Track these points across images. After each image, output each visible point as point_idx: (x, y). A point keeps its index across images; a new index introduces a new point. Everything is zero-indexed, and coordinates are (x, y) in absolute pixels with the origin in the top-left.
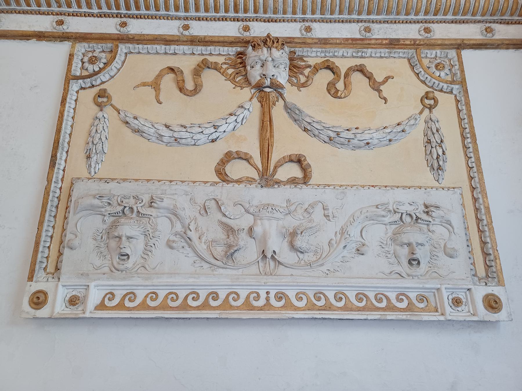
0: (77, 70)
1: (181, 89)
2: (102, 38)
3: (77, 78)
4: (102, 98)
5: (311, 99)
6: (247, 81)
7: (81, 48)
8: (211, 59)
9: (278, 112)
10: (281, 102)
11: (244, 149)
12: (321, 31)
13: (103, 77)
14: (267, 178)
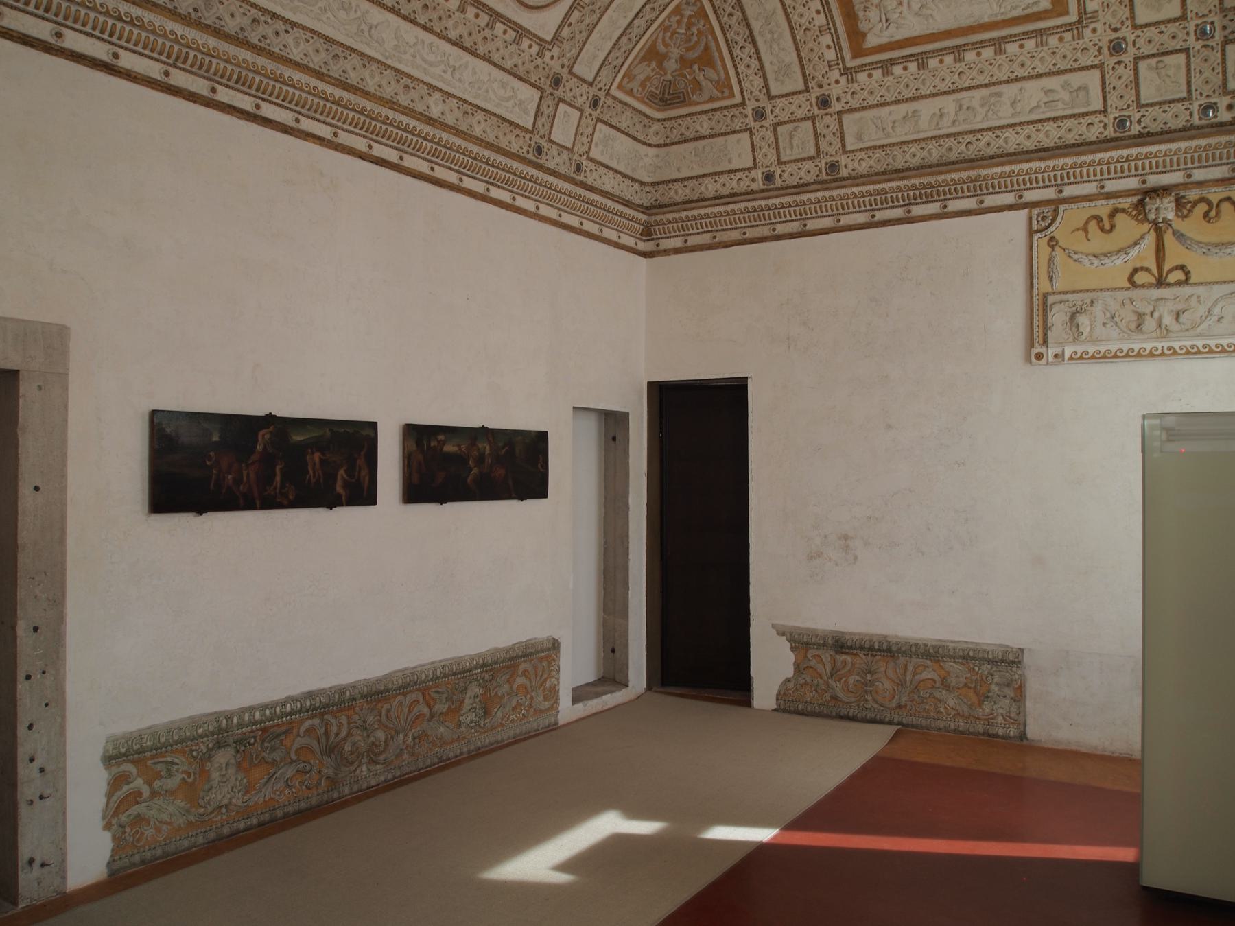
0: (1035, 227)
1: (1102, 229)
2: (1048, 202)
3: (1037, 232)
4: (1053, 242)
5: (1192, 226)
6: (1146, 219)
7: (1036, 211)
8: (1120, 206)
9: (1168, 238)
10: (1170, 231)
11: (1145, 264)
12: (1199, 175)
13: (1052, 229)
14: (1161, 283)
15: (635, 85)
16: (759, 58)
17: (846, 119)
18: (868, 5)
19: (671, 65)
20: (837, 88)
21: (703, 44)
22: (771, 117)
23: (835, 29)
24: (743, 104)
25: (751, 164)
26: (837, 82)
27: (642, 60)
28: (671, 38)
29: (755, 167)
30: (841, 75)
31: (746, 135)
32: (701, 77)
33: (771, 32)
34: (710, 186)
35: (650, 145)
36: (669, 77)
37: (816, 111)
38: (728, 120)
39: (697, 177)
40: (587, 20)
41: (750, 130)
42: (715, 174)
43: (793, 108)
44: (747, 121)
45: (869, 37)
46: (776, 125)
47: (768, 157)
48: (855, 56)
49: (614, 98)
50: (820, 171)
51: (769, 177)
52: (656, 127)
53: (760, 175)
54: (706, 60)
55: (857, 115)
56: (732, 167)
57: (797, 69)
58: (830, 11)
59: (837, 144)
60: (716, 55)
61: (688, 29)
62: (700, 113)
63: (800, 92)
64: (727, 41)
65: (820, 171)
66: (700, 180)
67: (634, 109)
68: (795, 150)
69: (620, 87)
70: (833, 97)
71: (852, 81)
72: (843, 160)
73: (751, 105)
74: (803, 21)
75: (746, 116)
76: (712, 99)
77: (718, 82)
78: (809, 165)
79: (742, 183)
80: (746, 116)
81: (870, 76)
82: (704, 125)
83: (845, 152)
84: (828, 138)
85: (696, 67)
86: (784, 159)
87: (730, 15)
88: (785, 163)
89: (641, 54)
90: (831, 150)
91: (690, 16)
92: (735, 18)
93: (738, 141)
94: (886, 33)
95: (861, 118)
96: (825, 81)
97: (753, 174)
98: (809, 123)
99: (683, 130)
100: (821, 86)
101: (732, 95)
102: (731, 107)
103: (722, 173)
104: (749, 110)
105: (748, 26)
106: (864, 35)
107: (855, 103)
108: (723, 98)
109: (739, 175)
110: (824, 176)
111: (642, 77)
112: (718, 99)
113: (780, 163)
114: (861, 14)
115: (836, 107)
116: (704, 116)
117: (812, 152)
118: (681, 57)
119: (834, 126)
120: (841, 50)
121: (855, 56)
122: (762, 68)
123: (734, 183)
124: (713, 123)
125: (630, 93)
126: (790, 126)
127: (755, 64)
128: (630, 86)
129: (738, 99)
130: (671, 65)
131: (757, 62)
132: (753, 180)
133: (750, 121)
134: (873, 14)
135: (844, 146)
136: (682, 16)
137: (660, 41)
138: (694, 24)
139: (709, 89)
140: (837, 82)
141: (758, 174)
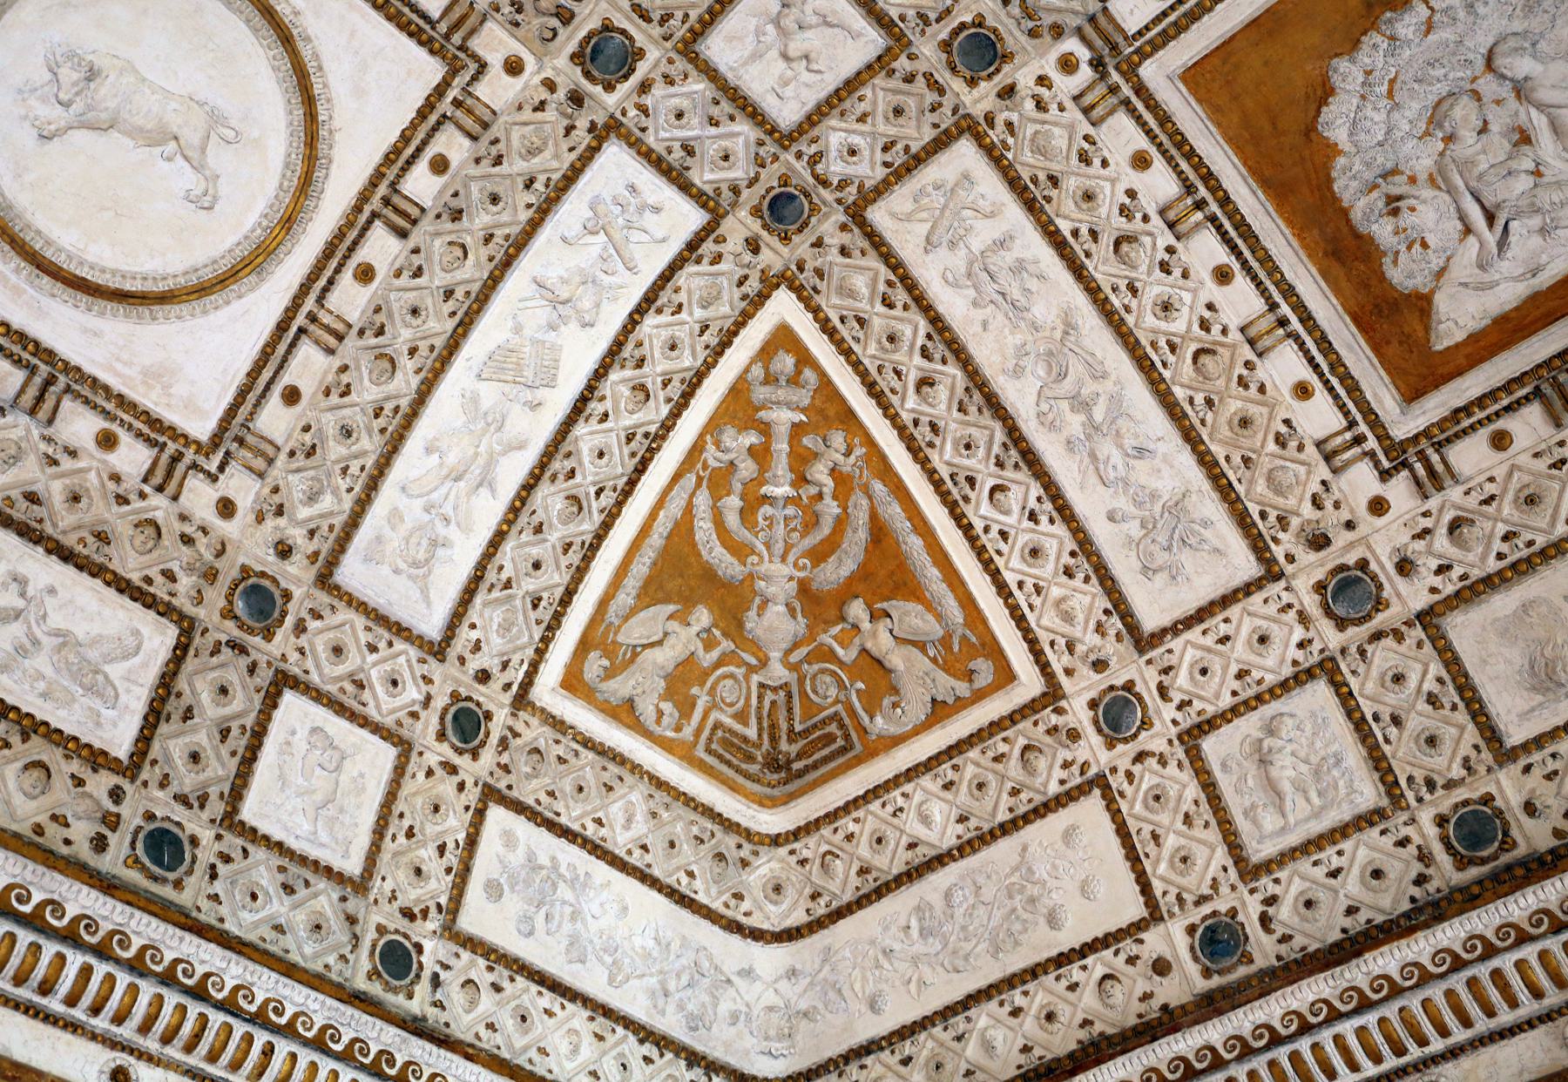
15: (643, 684)
16: (1064, 512)
17: (1462, 628)
18: (1398, 186)
19: (776, 625)
20: (1388, 524)
21: (861, 517)
22: (1169, 711)
23: (1307, 318)
24: (1052, 696)
25: (1135, 909)
26: (1378, 506)
27: (651, 593)
28: (747, 514)
29: (1155, 915)
30: (1385, 475)
31: (1091, 808)
32: (881, 641)
33: (1082, 405)
34: (999, 1036)
35: (757, 935)
36: (778, 672)
37: (1330, 637)
38: (1013, 767)
39: (946, 1014)
40: (367, 392)
41: (1101, 782)
42: (1011, 982)
43: (1240, 651)
44: (1081, 752)
45: (1442, 302)
46: (1192, 737)
47: (1194, 863)
48: (1412, 394)
49: (558, 725)
50: (1424, 857)
51: (1218, 940)
52: (768, 865)
53: (1182, 942)
54: (887, 576)
55: (1502, 603)
56: (1068, 939)
57: (1211, 507)
58: (1266, 260)
59: (1461, 735)
60: (914, 545)
61: (801, 480)
62: (911, 774)
63: (1248, 589)
64: (938, 484)
65: (1424, 857)
66: (959, 1022)
67: (660, 784)
68: (1297, 807)
69: (572, 682)
70: (1383, 564)
71: (1433, 481)
72: (1509, 788)
73: (1081, 691)
74: (1178, 325)
75: (1074, 735)
76: (940, 711)
77: (946, 641)
78: (1363, 850)
79: (1117, 992)
80: (1074, 735)
81: (1500, 441)
82: (933, 817)
83: (1505, 756)
84: (1413, 723)
85: (857, 610)
86: (1259, 851)
87: (925, 382)
88: (1267, 867)
89: (641, 568)
90: (1445, 763)
91: (797, 430)
92: (941, 393)
93: (1068, 835)
94: (1505, 267)
95: (1526, 607)
96: (1331, 519)
97: (1154, 942)
98: (1320, 691)
99: (864, 850)
100: (1319, 542)
101: (1006, 676)
102: (1013, 718)
103: (1034, 972)
104: (1078, 712)
105: (994, 405)
106: (1422, 304)
107: (1478, 561)
108: (979, 696)
109: (1098, 964)
110: (1447, 874)
111: (665, 657)
112: (961, 704)
113: (1249, 871)
114: (1383, 231)
115: (1411, 596)
116: (926, 781)
117: (1368, 794)
118: (804, 588)
119: (1426, 671)
120: (1354, 388)
121: (1412, 394)
122: (1084, 544)
123: (1088, 999)
124: (963, 795)
125: (625, 713)
126: (1248, 725)
127: (1055, 538)
128: (619, 687)
129: (1029, 683)
130: (776, 625)
131: (1060, 529)
132: (1161, 967)
133: (1093, 751)
134: (1431, 215)
135: (1491, 734)
136: (765, 429)
137: (704, 529)
138: (816, 455)
139: (919, 678)
140: (1378, 506)
141: (1172, 938)
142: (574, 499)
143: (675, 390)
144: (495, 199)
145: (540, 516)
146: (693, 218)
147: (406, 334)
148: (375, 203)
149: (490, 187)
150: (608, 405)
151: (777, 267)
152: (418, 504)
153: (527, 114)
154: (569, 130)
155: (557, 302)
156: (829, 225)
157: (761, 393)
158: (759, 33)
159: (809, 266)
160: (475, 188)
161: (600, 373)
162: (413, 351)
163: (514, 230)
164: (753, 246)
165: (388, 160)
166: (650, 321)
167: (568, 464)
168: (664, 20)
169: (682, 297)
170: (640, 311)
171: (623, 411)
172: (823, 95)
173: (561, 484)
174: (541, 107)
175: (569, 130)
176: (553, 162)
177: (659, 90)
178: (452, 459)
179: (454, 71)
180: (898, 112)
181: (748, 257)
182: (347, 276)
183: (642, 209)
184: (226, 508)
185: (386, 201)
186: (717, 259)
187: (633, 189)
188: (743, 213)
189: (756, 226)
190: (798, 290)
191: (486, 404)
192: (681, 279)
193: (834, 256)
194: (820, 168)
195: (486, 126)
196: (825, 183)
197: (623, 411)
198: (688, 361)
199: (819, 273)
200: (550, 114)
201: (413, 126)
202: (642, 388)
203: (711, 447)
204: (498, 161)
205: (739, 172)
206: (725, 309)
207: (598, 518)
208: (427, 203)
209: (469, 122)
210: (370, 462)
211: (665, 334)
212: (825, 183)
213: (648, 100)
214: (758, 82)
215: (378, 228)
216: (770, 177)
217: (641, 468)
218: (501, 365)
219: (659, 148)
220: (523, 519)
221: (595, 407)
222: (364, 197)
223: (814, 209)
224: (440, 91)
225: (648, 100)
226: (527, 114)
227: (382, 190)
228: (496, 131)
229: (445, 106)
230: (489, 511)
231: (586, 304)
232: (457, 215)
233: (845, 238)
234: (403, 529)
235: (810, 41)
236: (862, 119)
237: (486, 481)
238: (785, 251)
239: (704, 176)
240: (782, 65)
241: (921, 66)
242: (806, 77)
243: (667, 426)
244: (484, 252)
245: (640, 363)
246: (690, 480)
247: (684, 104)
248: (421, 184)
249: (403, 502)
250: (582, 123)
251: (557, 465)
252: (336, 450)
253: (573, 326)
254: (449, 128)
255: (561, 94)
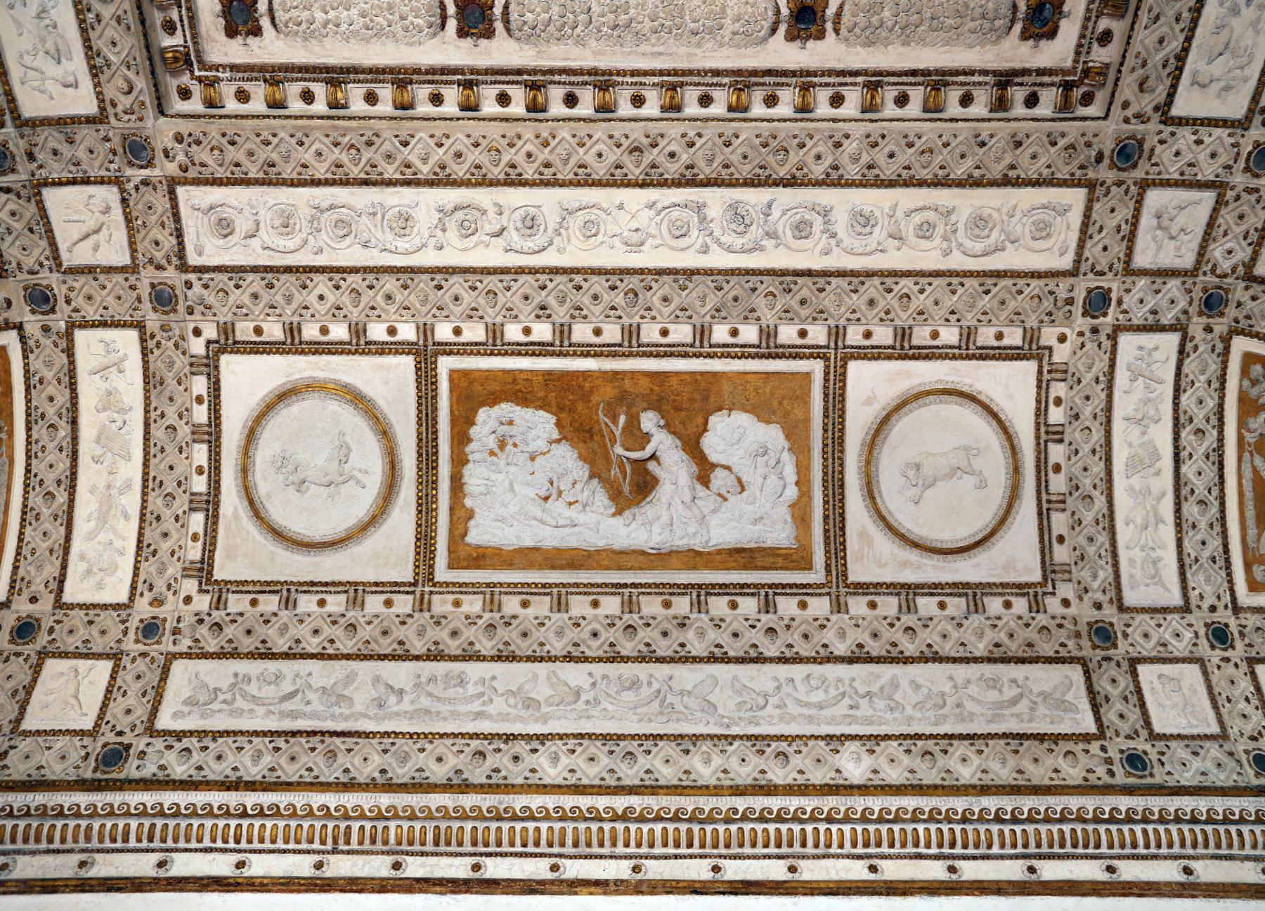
142: (1201, 502)
143: (1214, 421)
144: (1088, 398)
145: (1191, 520)
146: (1173, 339)
147: (1088, 482)
148: (1043, 437)
149: (1083, 395)
150: (1189, 449)
151: (1225, 329)
152: (1137, 550)
153: (1079, 353)
154: (1099, 346)
155: (1139, 421)
156: (1239, 292)
157: (1254, 392)
158: (1154, 238)
159: (1241, 317)
160: (1077, 400)
161: (1176, 438)
162: (1095, 487)
163: (1103, 405)
164: (1208, 329)
165: (1037, 415)
166: (1184, 398)
167: (1188, 488)
168: (1110, 269)
169: (1191, 377)
170: (1176, 397)
171: (1198, 448)
172: (1199, 239)
173: (1191, 499)
174: (1083, 345)
175: (1099, 346)
176: (1101, 365)
177: (1126, 299)
178: (1139, 521)
179: (1040, 360)
180: (1241, 217)
181: (1209, 336)
182: (1051, 473)
183: (1150, 354)
184: (1066, 603)
185: (1047, 433)
186: (1196, 348)
187: (1141, 348)
188: (1195, 319)
189: (1204, 320)
190: (1242, 332)
191: (1137, 487)
192: (1186, 369)
193: (1250, 304)
194: (1218, 272)
195: (1066, 372)
196: (1225, 276)
197: (1198, 448)
198: (1211, 403)
199: (1248, 317)
200: (1089, 345)
201: (1038, 394)
202: (1199, 430)
203: (1246, 434)
204: (1079, 381)
205: (1182, 304)
206: (1214, 367)
207: (1216, 503)
208: (1062, 421)
209: (1059, 376)
210: (1107, 546)
211: (1193, 399)
212: (1225, 276)
213: (1125, 306)
214: (1167, 259)
215: (1051, 446)
216: (1198, 294)
217: (1221, 467)
218: (1134, 465)
219: (1141, 322)
220: (1185, 526)
221: (1184, 454)
222: (1038, 437)
223: (1227, 291)
224: (1040, 372)
225: (1125, 306)
226: (1079, 353)
227: (1043, 429)
228: (1071, 370)
229: (1046, 376)
230: (1168, 533)
231: (1152, 412)
232: (1077, 417)
233: (1251, 292)
234: (1138, 565)
235: (1181, 221)
236: (1225, 234)
237: (1160, 521)
238: (1224, 320)
239: (1167, 318)
240: (1173, 243)
241: (1240, 188)
242: (1187, 238)
243: (1221, 439)
244: (1097, 423)
245: (1191, 420)
246: (1247, 455)
247: (1140, 295)
248: (1056, 415)
249: (1131, 554)
250: (1103, 338)
251: (1184, 492)
252: (1091, 550)
253: (1152, 426)
254: (1053, 384)
255: (1088, 334)
